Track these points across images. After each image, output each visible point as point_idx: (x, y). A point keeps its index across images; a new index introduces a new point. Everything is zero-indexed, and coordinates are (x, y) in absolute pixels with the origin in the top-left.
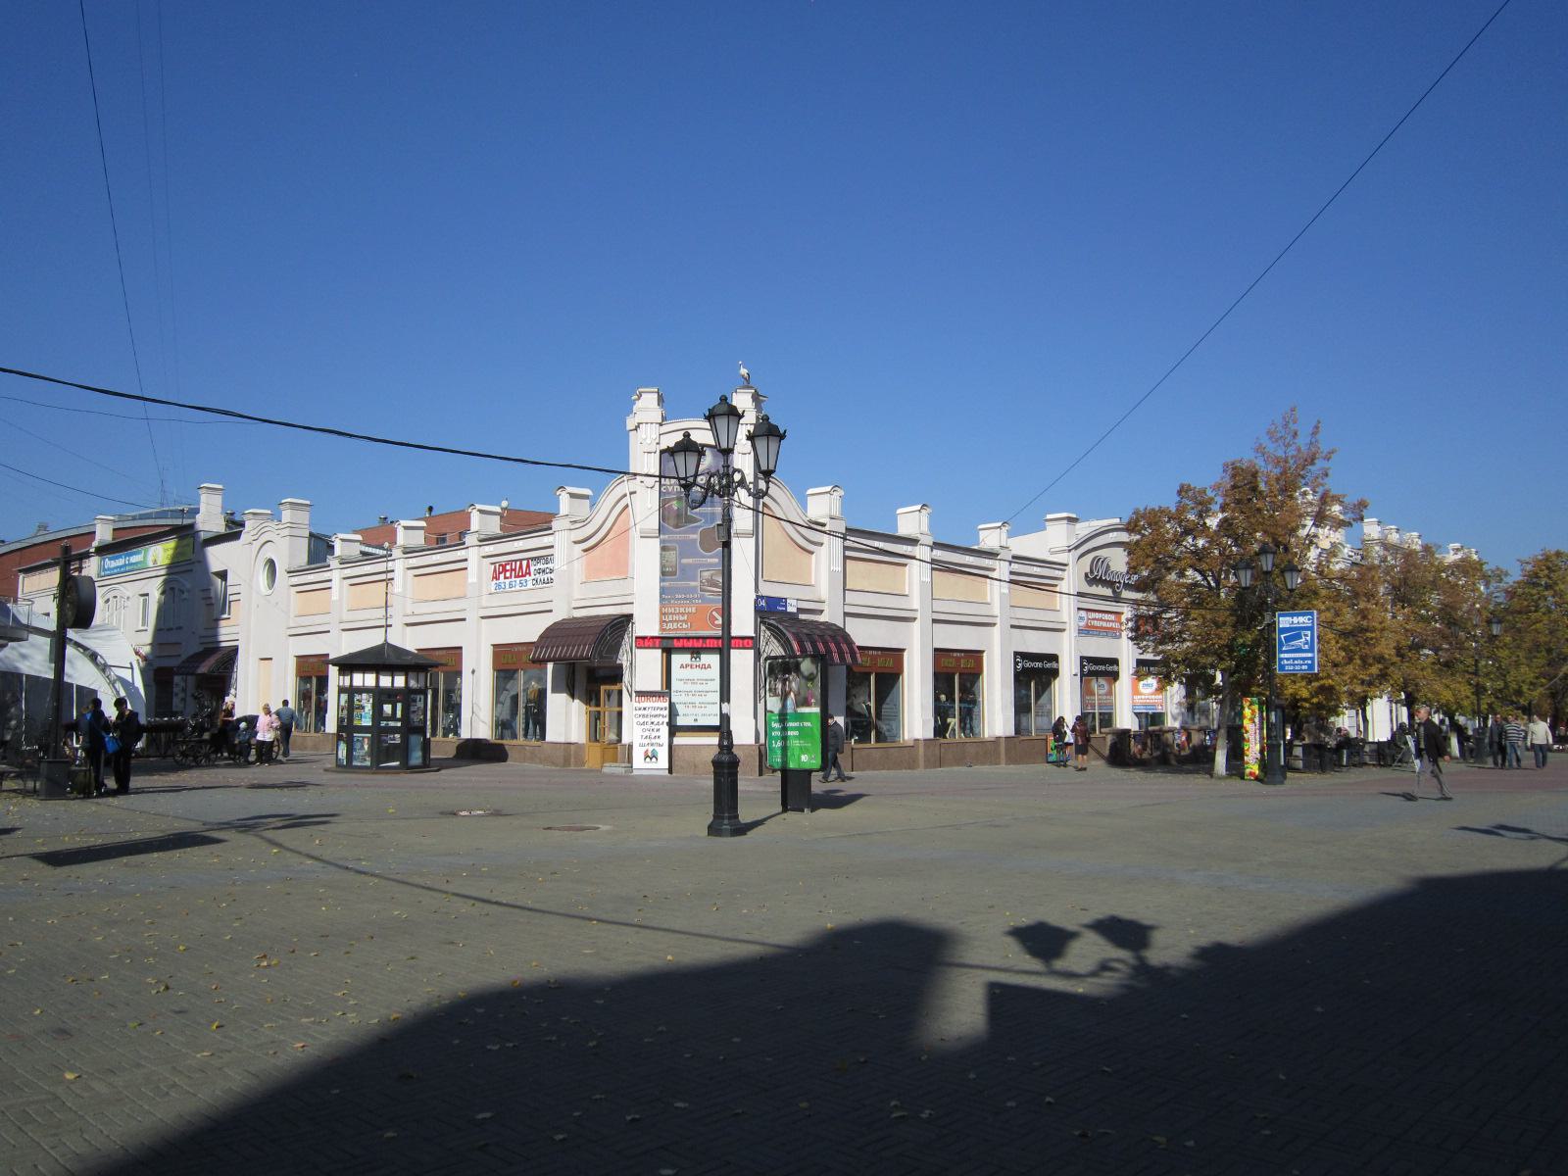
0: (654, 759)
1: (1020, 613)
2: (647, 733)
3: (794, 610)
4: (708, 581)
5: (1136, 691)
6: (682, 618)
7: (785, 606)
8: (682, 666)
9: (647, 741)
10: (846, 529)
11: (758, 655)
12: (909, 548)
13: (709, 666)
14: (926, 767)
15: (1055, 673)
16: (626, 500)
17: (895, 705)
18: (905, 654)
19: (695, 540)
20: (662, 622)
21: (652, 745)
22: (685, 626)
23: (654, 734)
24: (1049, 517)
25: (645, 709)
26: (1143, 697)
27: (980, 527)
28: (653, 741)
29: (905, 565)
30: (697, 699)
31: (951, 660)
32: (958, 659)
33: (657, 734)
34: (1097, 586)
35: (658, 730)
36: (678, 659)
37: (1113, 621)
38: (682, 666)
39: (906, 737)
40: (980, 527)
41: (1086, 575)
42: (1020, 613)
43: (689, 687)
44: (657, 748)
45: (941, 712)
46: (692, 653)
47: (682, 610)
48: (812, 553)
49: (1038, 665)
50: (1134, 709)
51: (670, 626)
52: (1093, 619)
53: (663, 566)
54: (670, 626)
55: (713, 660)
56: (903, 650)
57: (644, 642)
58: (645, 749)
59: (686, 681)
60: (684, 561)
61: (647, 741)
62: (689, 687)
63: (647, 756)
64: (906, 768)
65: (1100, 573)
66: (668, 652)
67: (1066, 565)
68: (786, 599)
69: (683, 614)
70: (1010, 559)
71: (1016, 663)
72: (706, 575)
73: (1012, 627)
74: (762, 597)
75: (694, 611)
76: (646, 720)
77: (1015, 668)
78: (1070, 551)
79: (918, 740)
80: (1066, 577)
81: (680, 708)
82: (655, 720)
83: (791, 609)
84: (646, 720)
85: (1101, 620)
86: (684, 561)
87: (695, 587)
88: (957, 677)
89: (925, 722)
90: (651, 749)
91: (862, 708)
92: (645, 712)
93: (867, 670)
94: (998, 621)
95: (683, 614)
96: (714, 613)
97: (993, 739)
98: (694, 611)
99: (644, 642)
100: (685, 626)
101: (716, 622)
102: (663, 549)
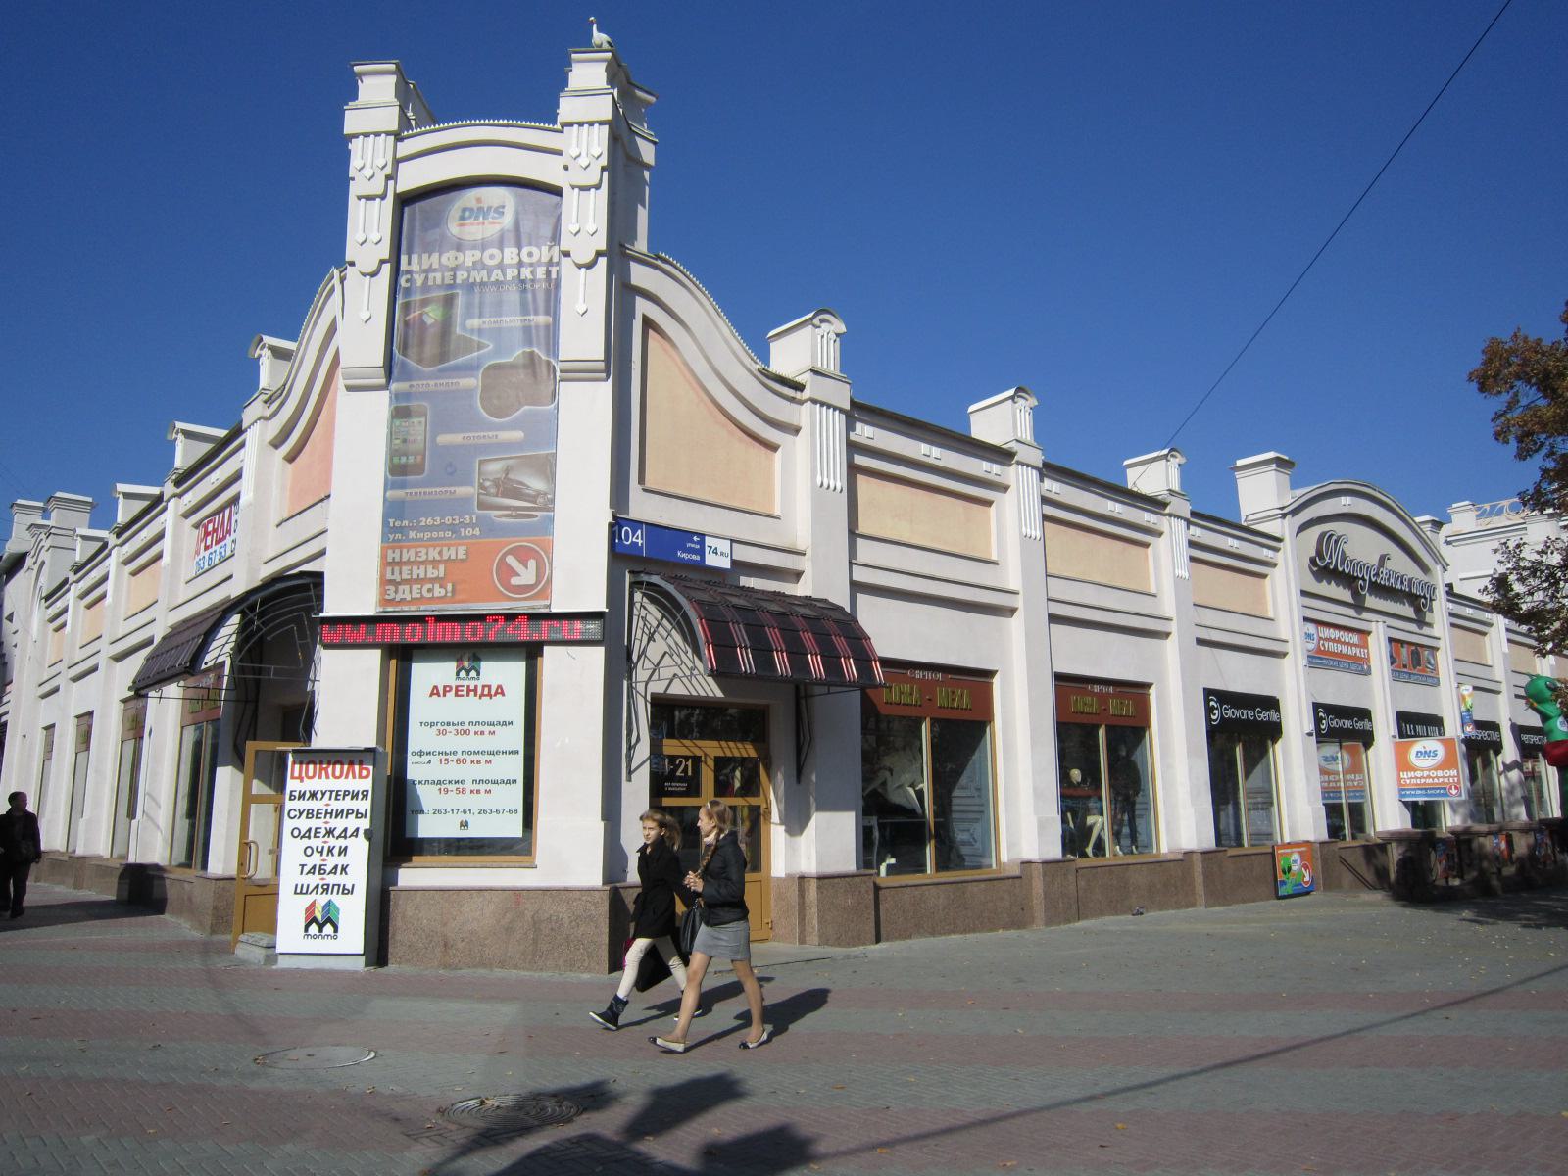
0: (328, 929)
1: (1210, 618)
2: (316, 859)
3: (725, 564)
4: (496, 483)
5: (1403, 764)
6: (432, 573)
7: (701, 552)
8: (435, 692)
9: (314, 880)
10: (852, 403)
11: (620, 666)
12: (996, 468)
13: (500, 691)
14: (1049, 922)
15: (1274, 731)
17: (979, 789)
18: (996, 681)
19: (469, 393)
20: (385, 582)
21: (326, 890)
22: (438, 592)
23: (332, 861)
24: (1240, 462)
25: (313, 795)
26: (1419, 774)
27: (1126, 462)
28: (331, 879)
29: (988, 503)
30: (468, 773)
31: (1088, 699)
32: (1103, 699)
33: (341, 861)
34: (1329, 583)
35: (343, 851)
36: (426, 675)
37: (1356, 645)
38: (435, 692)
39: (1004, 858)
40: (1126, 462)
41: (1313, 561)
42: (1210, 618)
43: (453, 742)
44: (338, 899)
45: (1074, 802)
46: (459, 660)
47: (434, 554)
48: (773, 447)
49: (1247, 714)
50: (1401, 795)
51: (404, 592)
52: (1329, 640)
53: (393, 453)
54: (404, 592)
55: (508, 673)
56: (990, 674)
57: (353, 631)
58: (307, 900)
59: (443, 727)
60: (444, 439)
61: (314, 880)
62: (453, 742)
63: (311, 921)
64: (1004, 927)
65: (1333, 560)
66: (401, 656)
68: (702, 536)
69: (435, 563)
70: (1188, 516)
71: (1209, 710)
72: (494, 468)
73: (1200, 642)
74: (636, 524)
75: (461, 555)
77: (1209, 720)
78: (1284, 516)
79: (1027, 864)
80: (1279, 558)
81: (427, 796)
82: (339, 824)
83: (716, 560)
84: (314, 823)
85: (1338, 641)
86: (444, 439)
87: (467, 500)
88: (1102, 734)
89: (1042, 826)
90: (322, 899)
91: (907, 795)
92: (314, 805)
93: (914, 713)
94: (1173, 627)
95: (435, 563)
96: (511, 560)
97: (1180, 857)
98: (461, 555)
99: (353, 631)
100: (438, 592)
101: (515, 581)
102: (400, 413)
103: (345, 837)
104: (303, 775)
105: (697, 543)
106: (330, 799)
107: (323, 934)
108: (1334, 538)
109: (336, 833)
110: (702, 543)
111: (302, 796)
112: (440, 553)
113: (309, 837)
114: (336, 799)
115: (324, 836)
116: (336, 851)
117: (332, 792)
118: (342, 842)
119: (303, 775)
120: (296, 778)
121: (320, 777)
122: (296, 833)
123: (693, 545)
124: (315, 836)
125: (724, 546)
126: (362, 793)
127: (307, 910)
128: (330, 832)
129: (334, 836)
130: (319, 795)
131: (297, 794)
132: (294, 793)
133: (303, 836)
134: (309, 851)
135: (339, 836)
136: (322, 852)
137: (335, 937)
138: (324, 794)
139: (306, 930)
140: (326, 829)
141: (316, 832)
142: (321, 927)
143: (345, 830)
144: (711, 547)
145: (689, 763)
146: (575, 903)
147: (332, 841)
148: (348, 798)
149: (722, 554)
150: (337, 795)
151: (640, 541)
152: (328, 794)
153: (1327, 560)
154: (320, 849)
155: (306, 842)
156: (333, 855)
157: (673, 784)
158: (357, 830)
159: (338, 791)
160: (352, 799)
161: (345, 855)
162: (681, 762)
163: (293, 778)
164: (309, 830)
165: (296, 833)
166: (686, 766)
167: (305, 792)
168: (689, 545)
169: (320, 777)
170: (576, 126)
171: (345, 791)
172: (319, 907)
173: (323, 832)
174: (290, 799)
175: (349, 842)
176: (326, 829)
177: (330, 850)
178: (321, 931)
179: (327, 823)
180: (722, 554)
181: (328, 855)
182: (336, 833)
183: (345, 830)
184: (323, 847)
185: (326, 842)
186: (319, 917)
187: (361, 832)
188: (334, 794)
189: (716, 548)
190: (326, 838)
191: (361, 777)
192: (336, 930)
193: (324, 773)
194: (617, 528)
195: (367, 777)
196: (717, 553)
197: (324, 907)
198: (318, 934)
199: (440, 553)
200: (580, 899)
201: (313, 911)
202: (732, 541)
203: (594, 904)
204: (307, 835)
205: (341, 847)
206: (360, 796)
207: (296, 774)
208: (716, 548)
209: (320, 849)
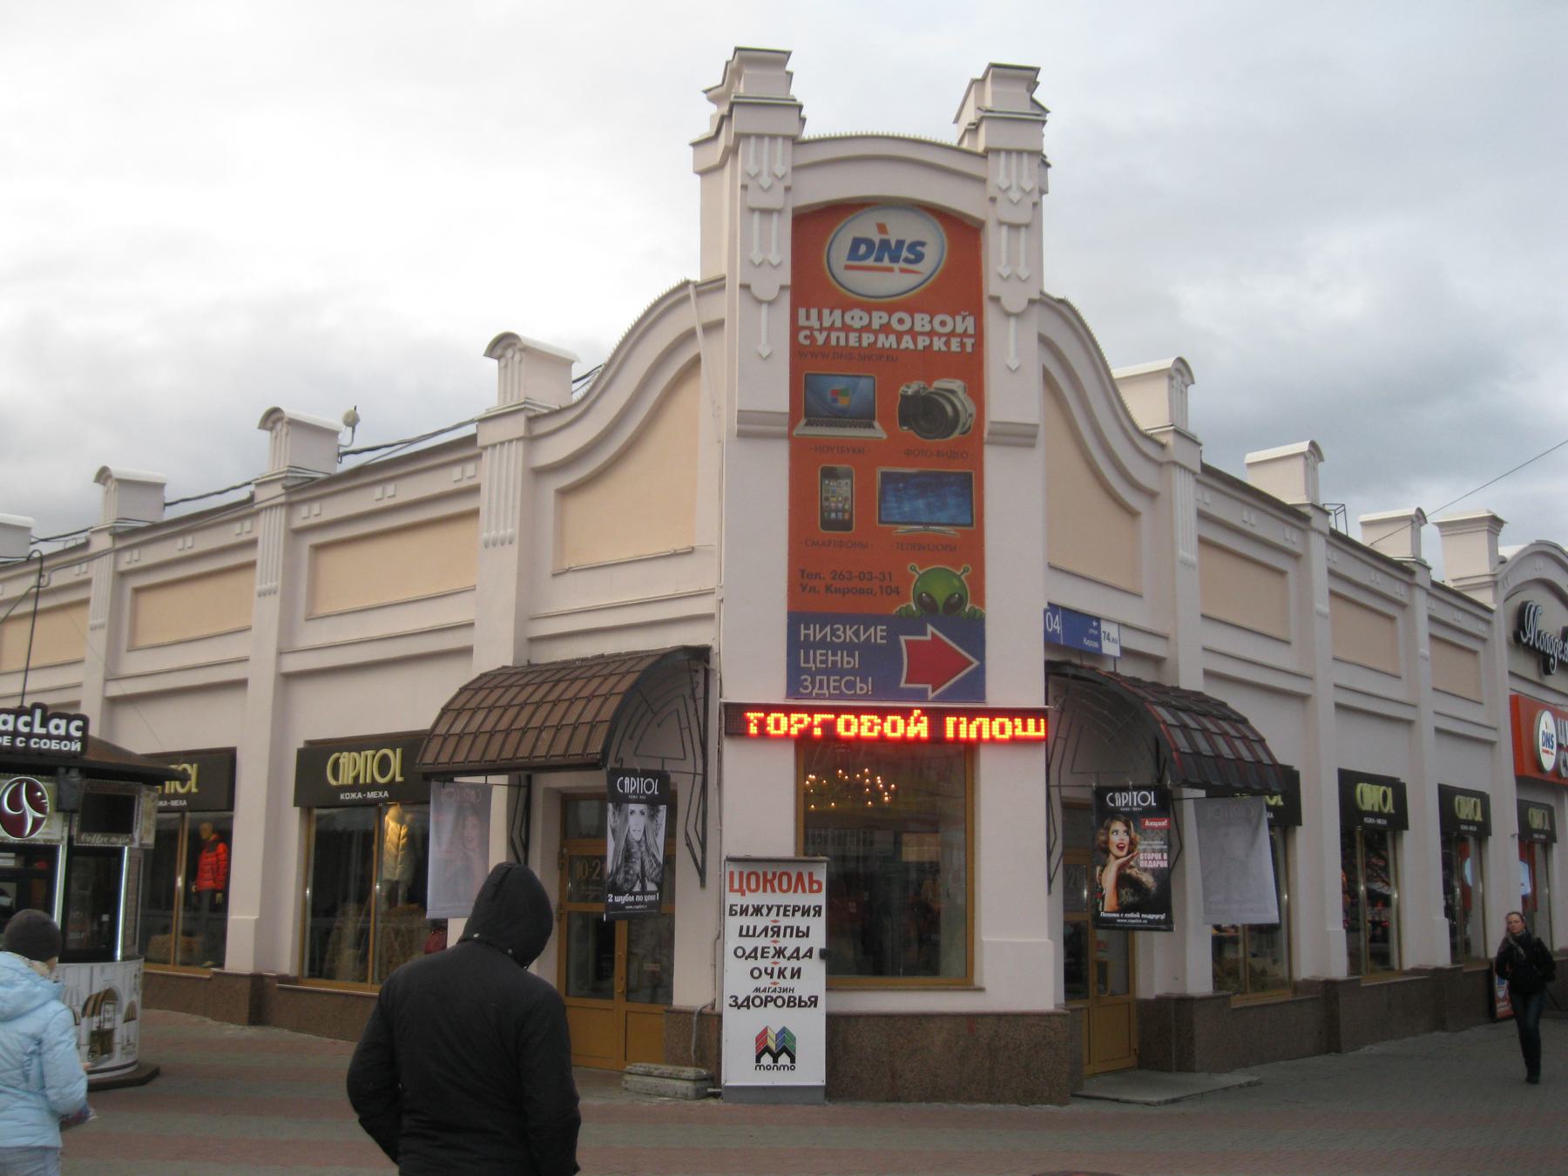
0: (784, 1059)
7: (1098, 639)
16: (700, 345)
25: (757, 910)
35: (796, 973)
67: (1489, 611)
68: (1098, 619)
70: (1428, 585)
76: (761, 942)
84: (761, 942)
103: (798, 958)
104: (745, 887)
106: (778, 915)
107: (779, 1065)
108: (1533, 609)
109: (788, 954)
110: (1098, 628)
111: (744, 911)
112: (857, 634)
113: (756, 958)
114: (785, 915)
115: (773, 957)
116: (788, 973)
117: (779, 907)
118: (794, 964)
119: (745, 887)
120: (737, 891)
121: (765, 891)
122: (740, 952)
124: (762, 957)
126: (814, 908)
127: (757, 1039)
128: (780, 952)
129: (784, 957)
130: (765, 911)
131: (738, 909)
132: (734, 908)
133: (749, 956)
134: (756, 973)
135: (791, 957)
136: (771, 975)
137: (792, 1068)
138: (770, 910)
139: (758, 1059)
140: (775, 948)
141: (763, 952)
142: (775, 1058)
143: (797, 950)
146: (1033, 1029)
147: (783, 963)
148: (798, 914)
149: (1113, 640)
150: (785, 910)
152: (775, 909)
153: (1528, 635)
154: (769, 971)
155: (752, 963)
156: (784, 977)
158: (811, 950)
159: (786, 907)
160: (803, 915)
161: (799, 977)
163: (732, 890)
164: (756, 950)
165: (740, 952)
167: (748, 907)
169: (765, 891)
170: (1003, 155)
171: (794, 907)
172: (772, 1035)
173: (772, 952)
174: (731, 915)
175: (803, 964)
176: (775, 948)
177: (781, 973)
178: (775, 1061)
179: (775, 942)
181: (779, 977)
182: (788, 954)
183: (797, 950)
184: (773, 969)
185: (775, 963)
186: (772, 1045)
187: (816, 953)
188: (782, 909)
190: (776, 959)
191: (811, 891)
192: (793, 1060)
193: (768, 885)
195: (819, 890)
197: (777, 1036)
198: (772, 1065)
199: (857, 634)
201: (766, 1039)
204: (753, 954)
205: (793, 969)
206: (812, 913)
207: (736, 886)
209: (769, 971)
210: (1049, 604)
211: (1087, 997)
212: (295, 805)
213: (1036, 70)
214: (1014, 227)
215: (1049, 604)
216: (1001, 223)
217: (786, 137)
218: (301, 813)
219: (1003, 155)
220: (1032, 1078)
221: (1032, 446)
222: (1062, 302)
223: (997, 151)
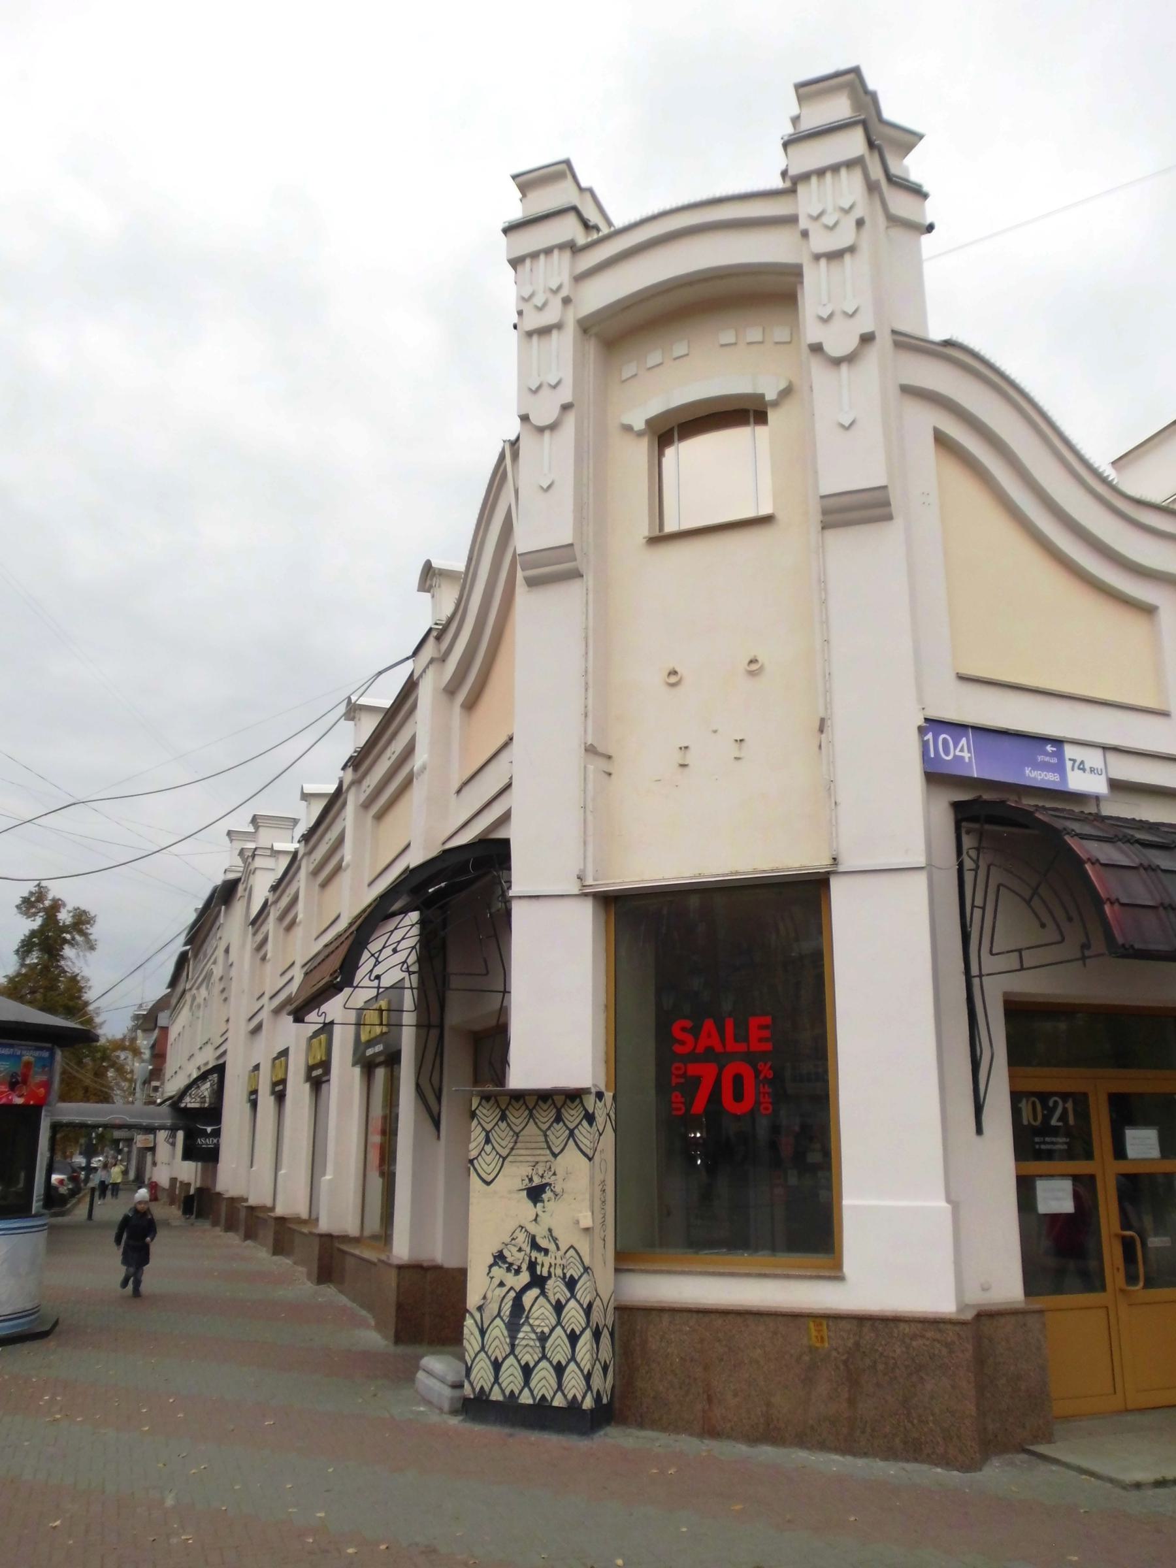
7: (1060, 768)
68: (1058, 742)
105: (1053, 754)
110: (1060, 755)
123: (1047, 759)
125: (1094, 758)
144: (1074, 761)
145: (1069, 1105)
146: (914, 1343)
149: (1092, 770)
151: (966, 755)
157: (1048, 1139)
162: (1056, 1103)
166: (1065, 1110)
168: (1040, 758)
180: (1092, 770)
189: (1082, 762)
194: (929, 736)
196: (1084, 770)
200: (923, 1336)
202: (1106, 748)
203: (947, 1345)
208: (1082, 762)
210: (926, 720)
211: (1103, 1288)
212: (354, 1065)
213: (856, 71)
214: (835, 256)
215: (926, 720)
216: (817, 257)
217: (561, 247)
218: (362, 1072)
219: (814, 180)
220: (915, 1421)
221: (889, 517)
222: (948, 343)
223: (805, 177)
